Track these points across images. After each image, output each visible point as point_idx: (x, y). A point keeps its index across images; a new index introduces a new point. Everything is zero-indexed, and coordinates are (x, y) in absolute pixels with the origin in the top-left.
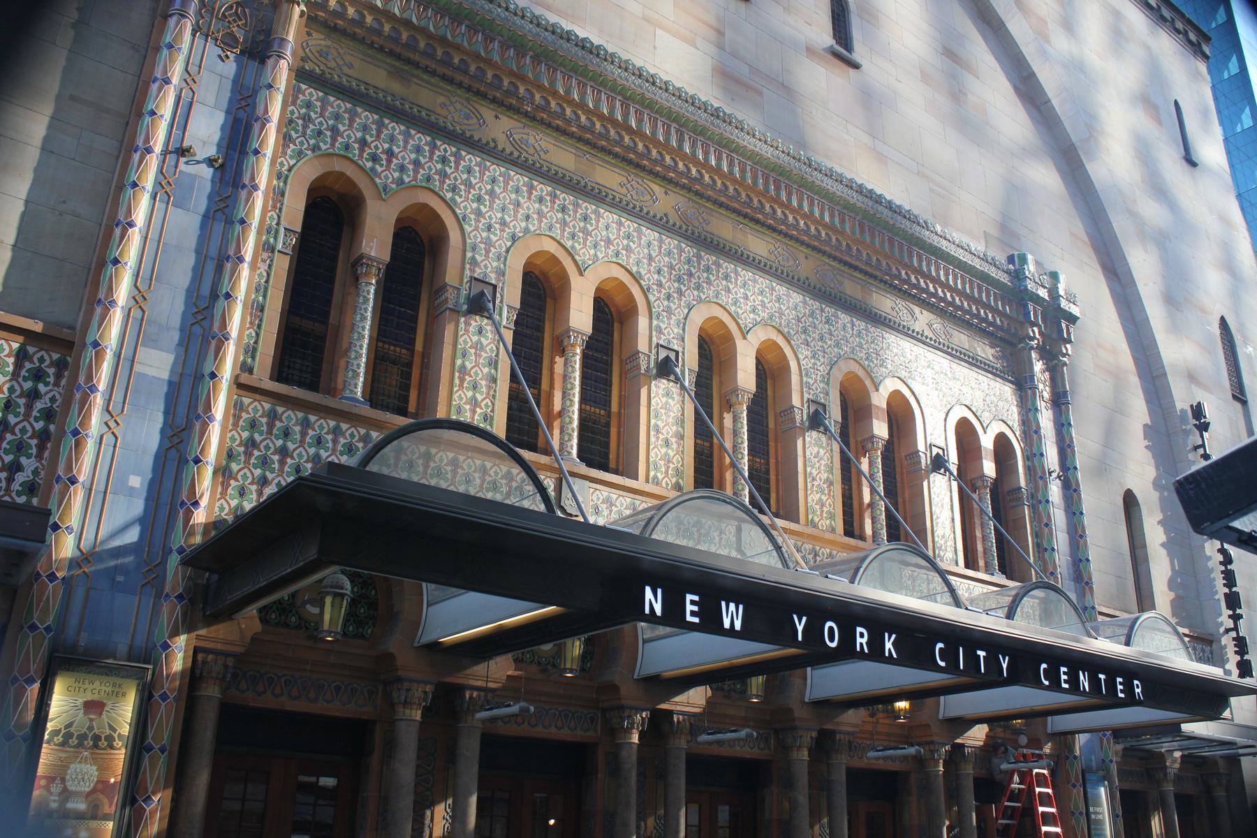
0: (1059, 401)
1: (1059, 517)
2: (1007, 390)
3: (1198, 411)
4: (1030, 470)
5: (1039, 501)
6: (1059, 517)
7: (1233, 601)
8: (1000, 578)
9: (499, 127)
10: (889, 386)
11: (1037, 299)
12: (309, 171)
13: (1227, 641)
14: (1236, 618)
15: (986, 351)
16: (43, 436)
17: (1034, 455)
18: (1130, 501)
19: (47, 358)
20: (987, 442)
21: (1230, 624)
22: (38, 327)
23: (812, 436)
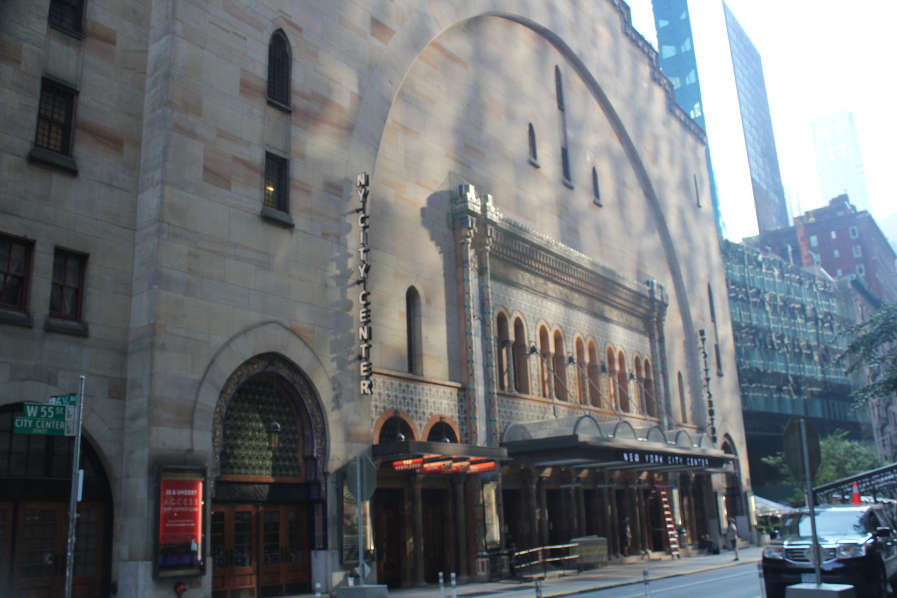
0: (661, 340)
1: (662, 388)
2: (647, 339)
3: (702, 333)
4: (654, 373)
5: (657, 384)
6: (662, 388)
7: (711, 413)
8: (648, 417)
9: (525, 278)
10: (619, 349)
11: (657, 301)
12: (496, 314)
13: (709, 429)
14: (712, 420)
15: (635, 321)
16: (465, 418)
17: (654, 366)
18: (680, 375)
19: (462, 393)
20: (643, 364)
21: (710, 422)
22: (459, 385)
23: (603, 374)
